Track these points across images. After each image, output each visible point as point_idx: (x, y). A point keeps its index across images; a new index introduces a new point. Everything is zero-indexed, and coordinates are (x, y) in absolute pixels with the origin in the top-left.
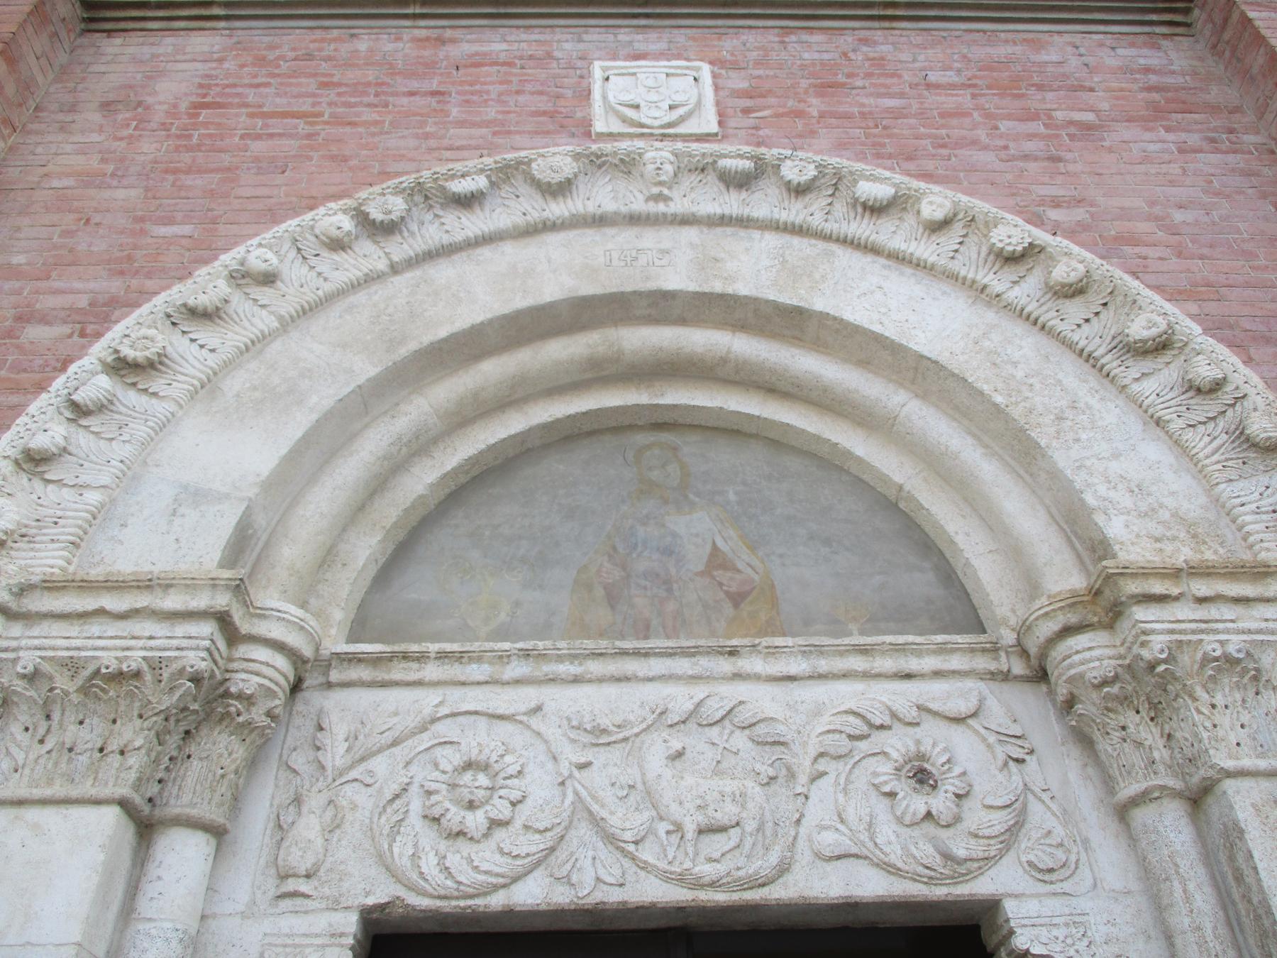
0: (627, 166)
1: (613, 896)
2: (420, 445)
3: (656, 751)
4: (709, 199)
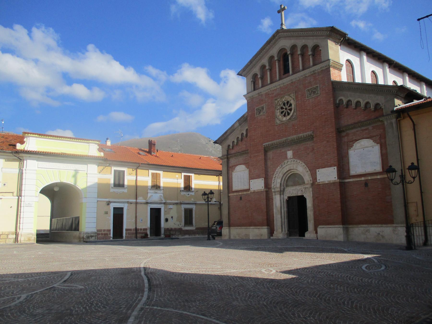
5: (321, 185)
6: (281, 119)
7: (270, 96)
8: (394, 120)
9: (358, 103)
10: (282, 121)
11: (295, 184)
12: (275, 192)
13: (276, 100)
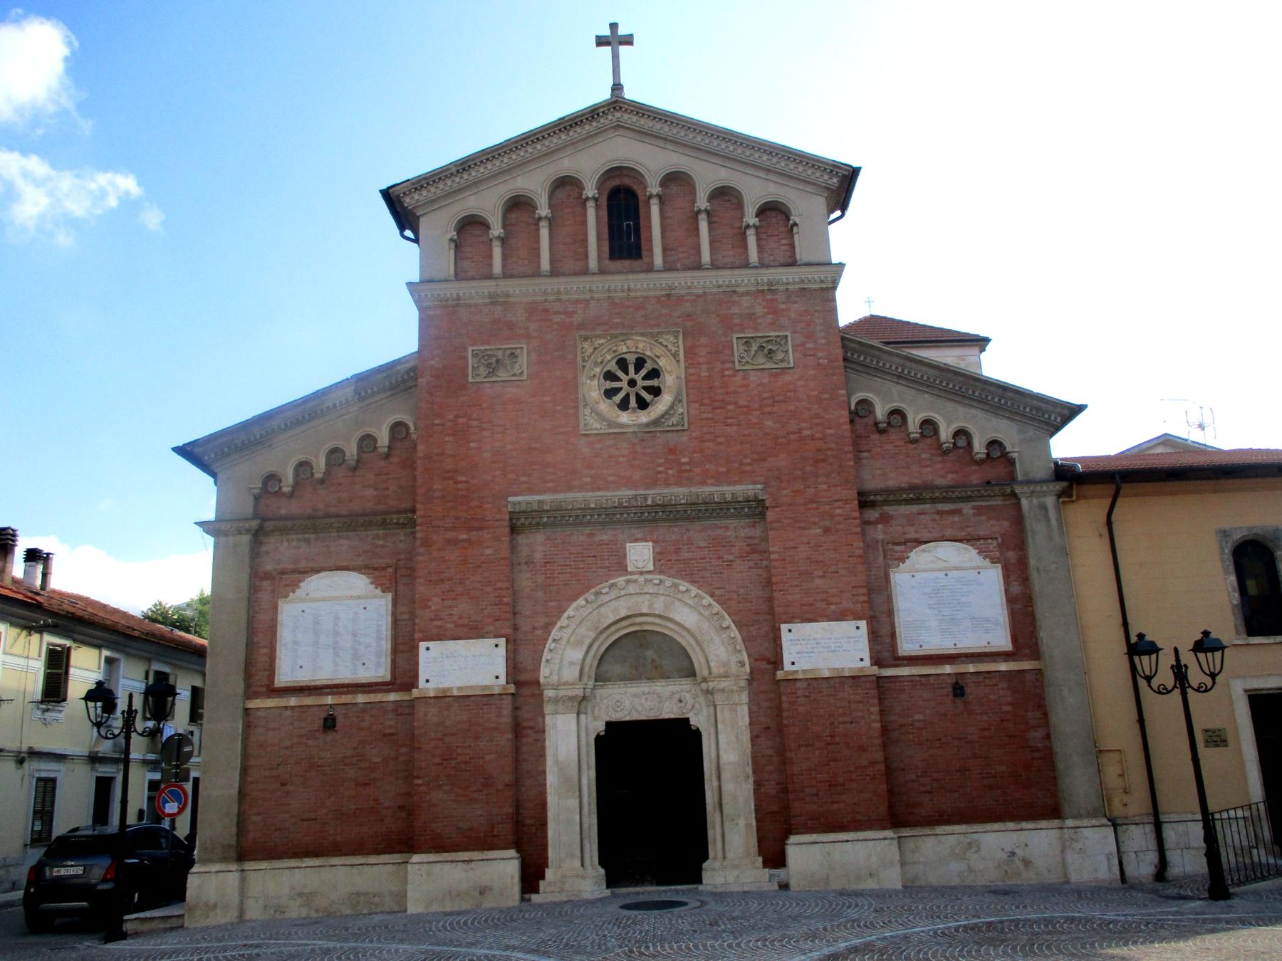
5: (799, 685)
6: (598, 411)
7: (556, 319)
8: (1050, 501)
9: (929, 425)
10: (611, 424)
11: (641, 672)
12: (556, 701)
13: (586, 339)
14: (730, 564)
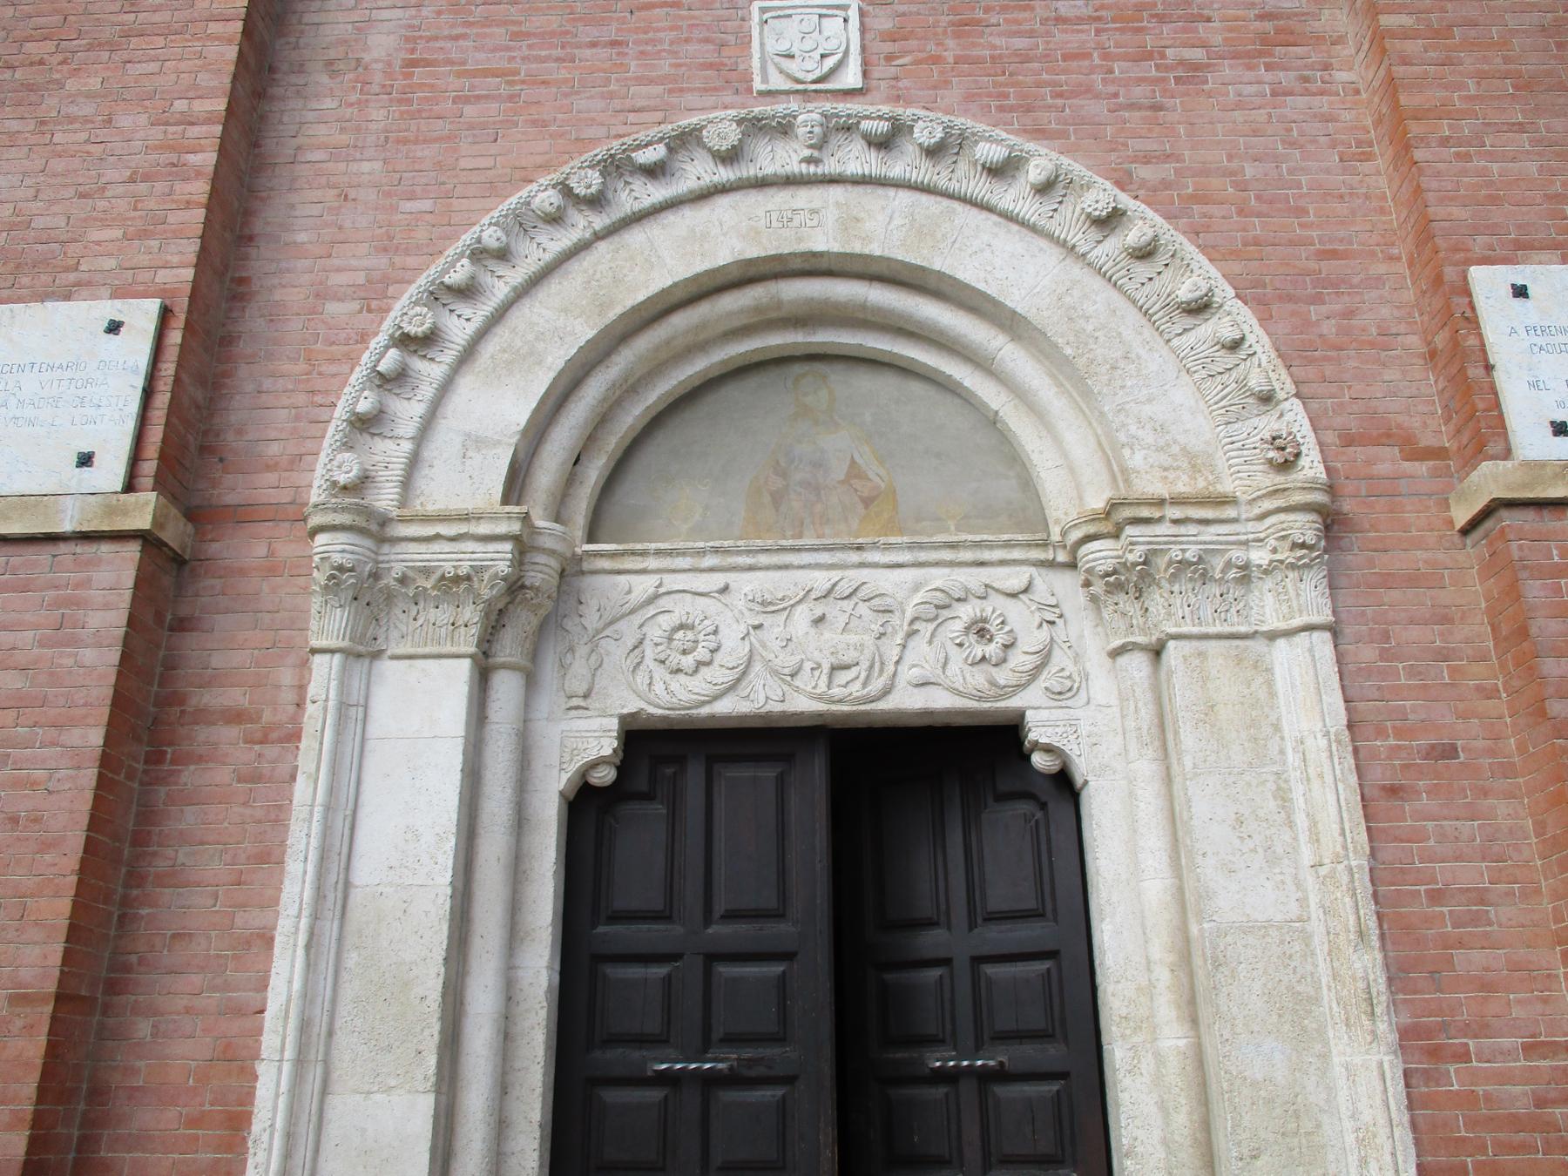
0: (784, 129)
1: (777, 708)
2: (629, 388)
3: (802, 616)
4: (854, 158)
14: (1193, 73)
